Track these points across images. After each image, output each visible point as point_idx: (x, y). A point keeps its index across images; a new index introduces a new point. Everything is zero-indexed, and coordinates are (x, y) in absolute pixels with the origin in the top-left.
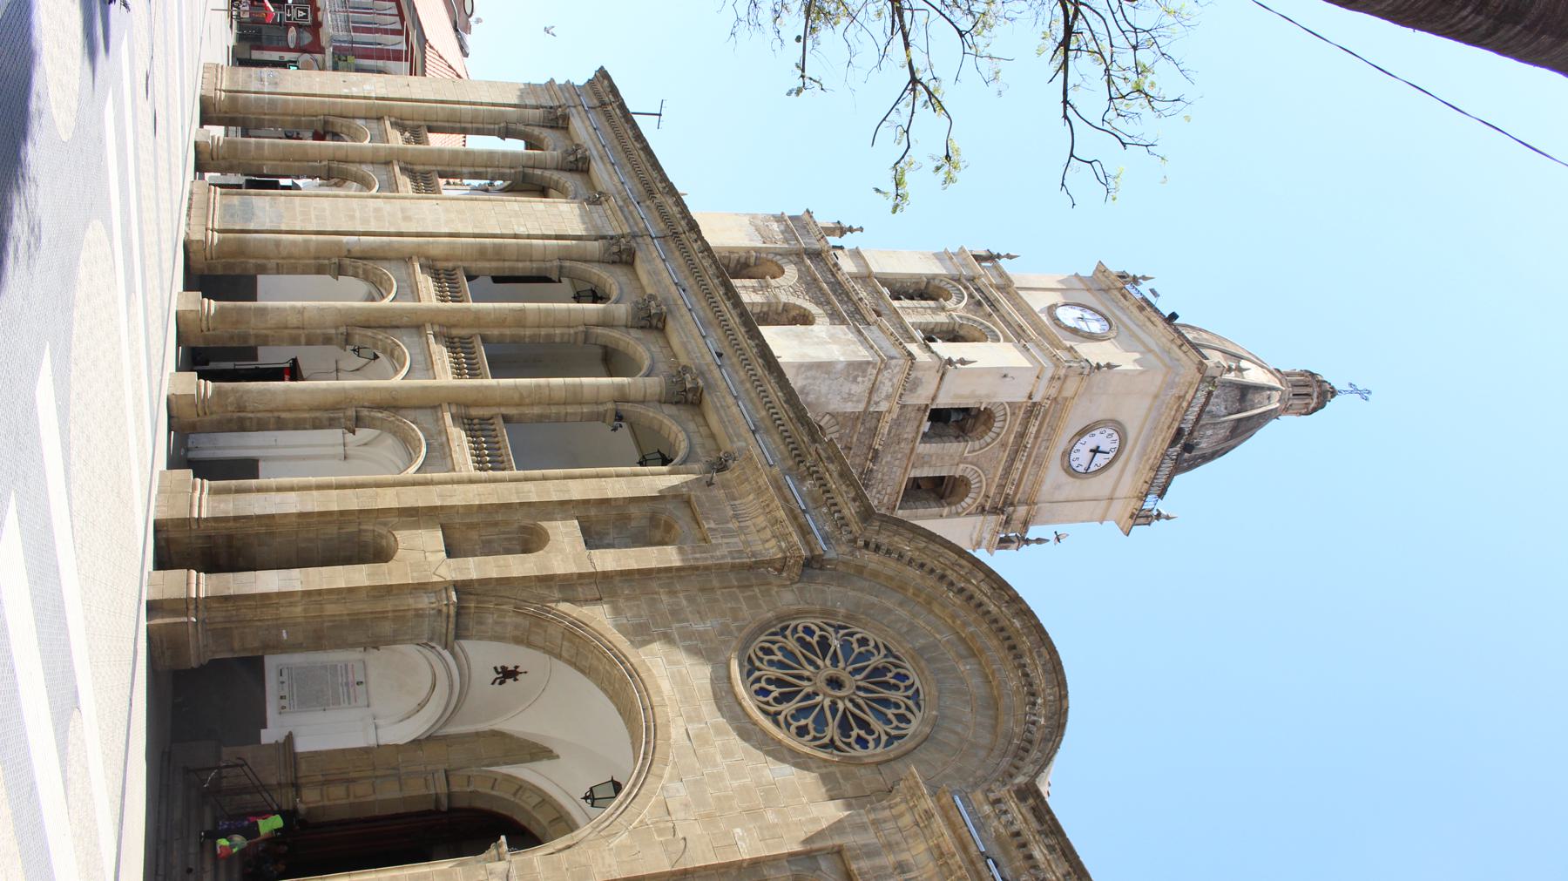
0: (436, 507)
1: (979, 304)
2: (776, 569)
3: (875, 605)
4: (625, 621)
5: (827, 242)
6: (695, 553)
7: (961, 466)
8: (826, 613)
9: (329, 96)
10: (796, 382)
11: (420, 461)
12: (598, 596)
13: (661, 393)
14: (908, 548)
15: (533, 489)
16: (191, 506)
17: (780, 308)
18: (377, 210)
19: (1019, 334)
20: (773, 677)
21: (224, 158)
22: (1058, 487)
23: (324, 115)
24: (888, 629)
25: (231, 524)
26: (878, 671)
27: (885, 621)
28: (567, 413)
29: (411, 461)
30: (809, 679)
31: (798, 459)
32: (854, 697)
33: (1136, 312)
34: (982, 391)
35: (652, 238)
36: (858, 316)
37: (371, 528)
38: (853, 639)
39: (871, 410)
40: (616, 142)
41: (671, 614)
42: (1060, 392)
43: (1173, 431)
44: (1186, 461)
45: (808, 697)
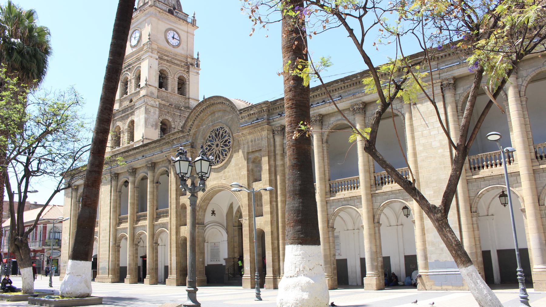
0: (176, 227)
3: (202, 133)
7: (175, 79)
9: (69, 248)
11: (166, 230)
17: (129, 128)
18: (103, 237)
19: (139, 59)
22: (183, 49)
25: (178, 271)
26: (216, 135)
29: (165, 231)
34: (154, 74)
36: (132, 107)
38: (209, 139)
42: (156, 50)
43: (169, 14)
44: (178, 8)
45: (219, 152)
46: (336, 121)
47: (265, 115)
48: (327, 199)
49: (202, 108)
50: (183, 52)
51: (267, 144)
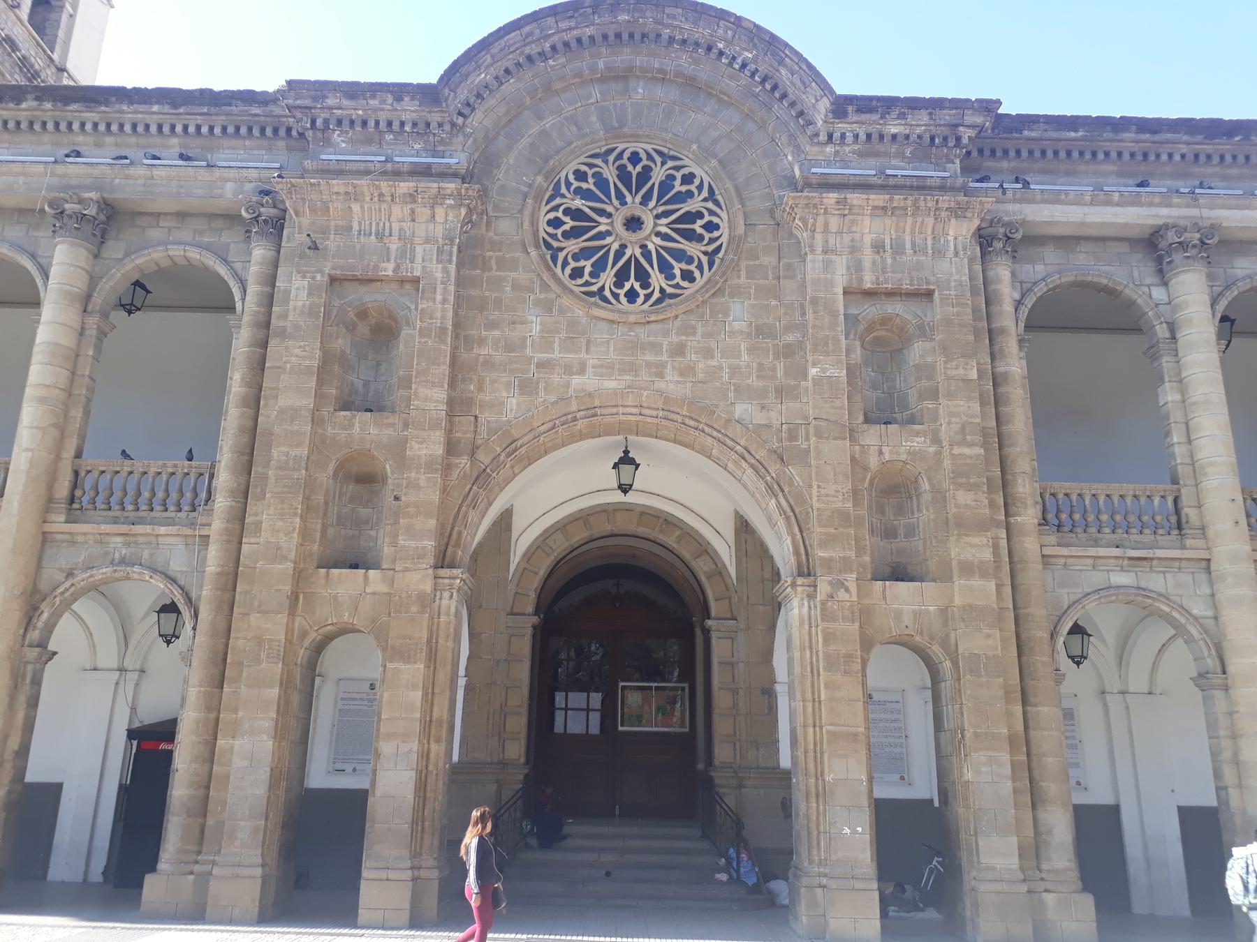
2: (467, 223)
3: (532, 144)
4: (514, 401)
6: (434, 300)
12: (473, 418)
13: (87, 249)
14: (483, 75)
15: (284, 449)
20: (615, 279)
24: (573, 146)
25: (269, 824)
26: (623, 175)
27: (560, 143)
30: (623, 247)
31: (282, 132)
32: (655, 212)
37: (303, 650)
41: (510, 352)
47: (954, 163)
51: (966, 278)
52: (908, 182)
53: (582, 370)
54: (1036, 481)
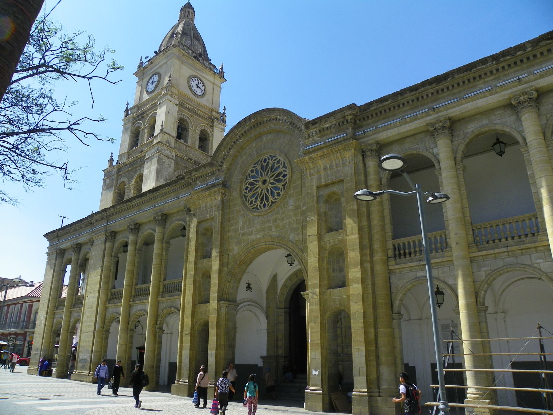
0: (192, 305)
1: (143, 117)
2: (225, 196)
5: (115, 165)
7: (197, 131)
8: (241, 182)
10: (162, 182)
12: (227, 255)
16: (184, 385)
17: (136, 184)
18: (87, 317)
19: (155, 106)
21: (63, 368)
22: (208, 100)
23: (51, 333)
25: (191, 372)
28: (165, 259)
30: (262, 190)
31: (189, 185)
32: (269, 177)
33: (153, 64)
34: (173, 121)
35: (108, 224)
36: (142, 159)
38: (251, 174)
39: (174, 158)
40: (72, 233)
44: (205, 57)
45: (268, 191)
46: (480, 127)
47: (349, 129)
48: (472, 255)
49: (243, 130)
50: (207, 104)
51: (353, 171)
52: (333, 142)
53: (251, 234)
54: (390, 240)
